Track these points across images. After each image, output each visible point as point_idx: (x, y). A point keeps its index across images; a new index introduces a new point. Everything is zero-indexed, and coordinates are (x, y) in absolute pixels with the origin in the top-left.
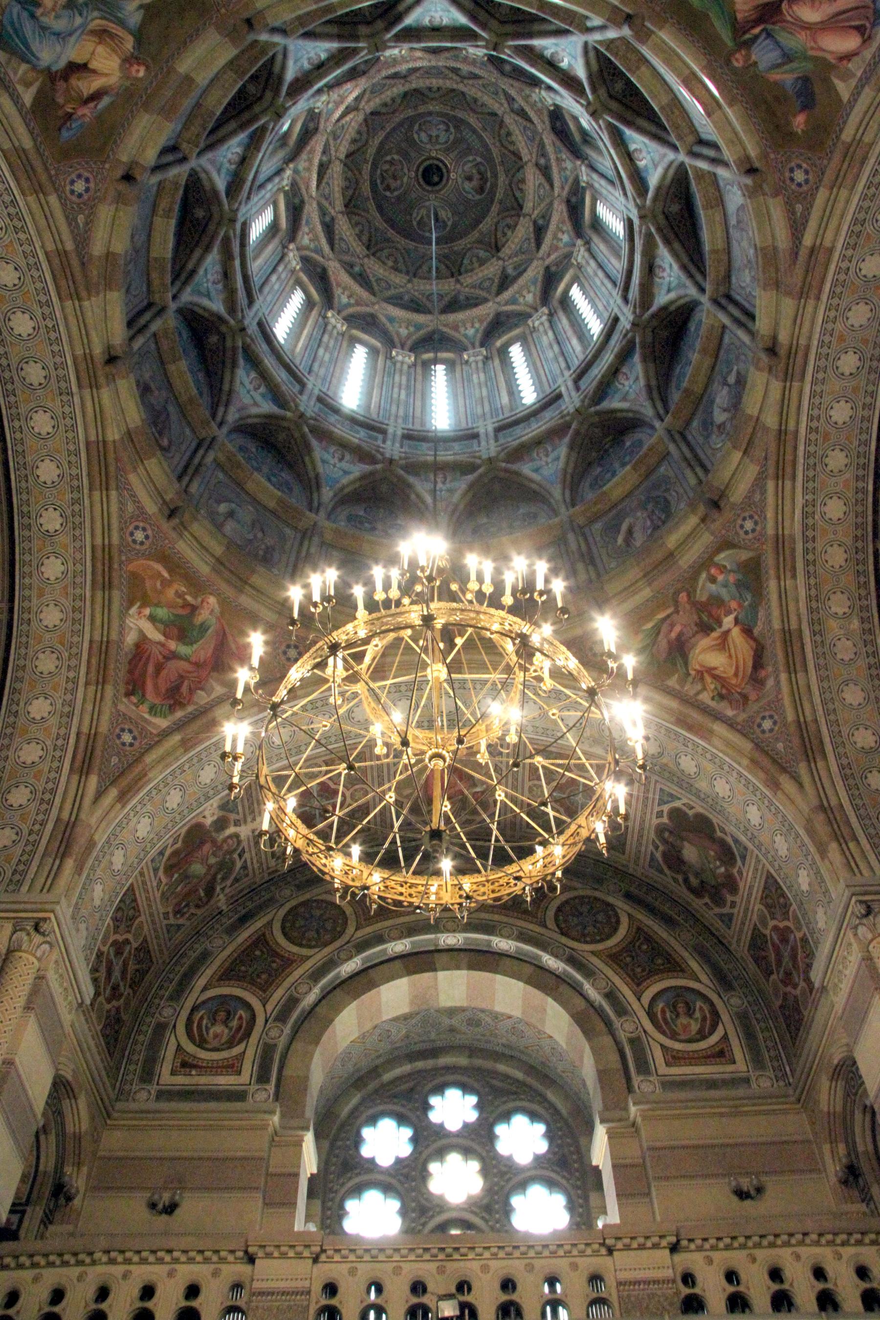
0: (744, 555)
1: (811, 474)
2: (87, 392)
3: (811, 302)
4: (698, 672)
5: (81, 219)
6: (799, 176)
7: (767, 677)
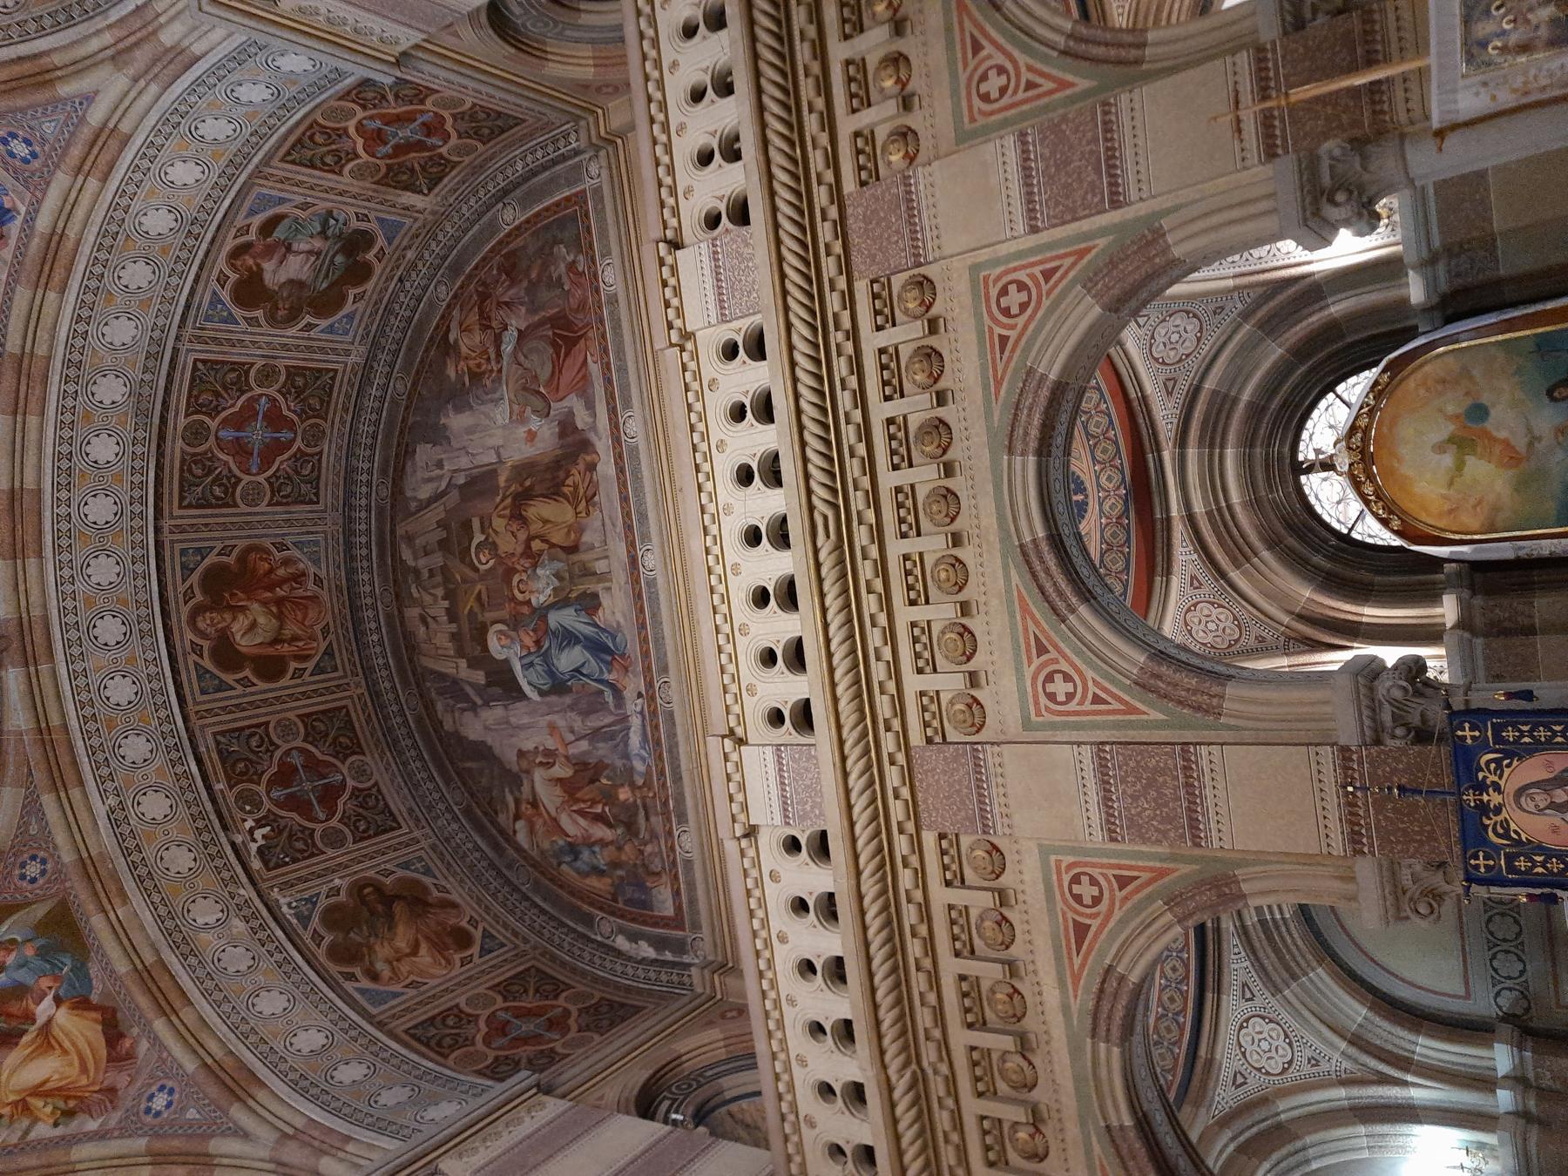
0: (40, 911)
1: (105, 771)
3: (32, 562)
4: (15, 1104)
7: (135, 1043)
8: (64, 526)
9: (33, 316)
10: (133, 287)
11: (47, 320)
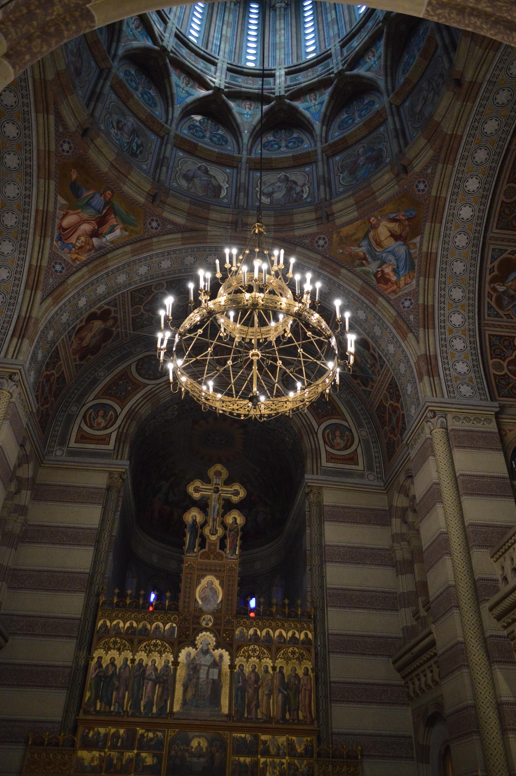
2: (479, 81)
3: (37, 77)
5: (429, 171)
6: (66, 147)
8: (24, 92)
9: (46, 199)
10: (10, 213)
11: (41, 195)
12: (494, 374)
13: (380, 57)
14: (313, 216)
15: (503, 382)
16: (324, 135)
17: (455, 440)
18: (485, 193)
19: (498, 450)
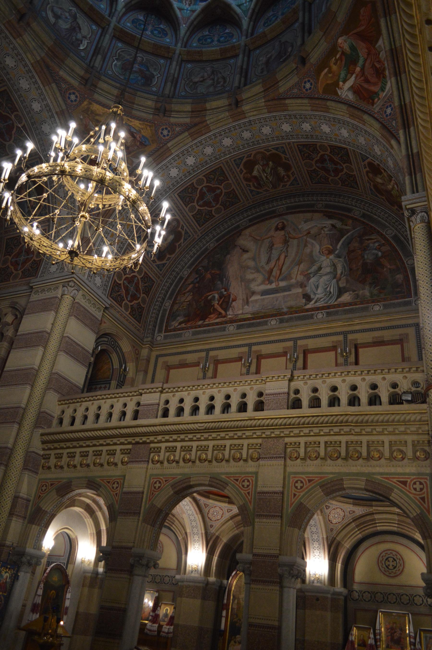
5: (178, 129)
12: (115, 280)
13: (193, 11)
14: (82, 73)
15: (116, 288)
16: (120, 15)
17: (78, 312)
18: (191, 172)
19: (95, 332)
